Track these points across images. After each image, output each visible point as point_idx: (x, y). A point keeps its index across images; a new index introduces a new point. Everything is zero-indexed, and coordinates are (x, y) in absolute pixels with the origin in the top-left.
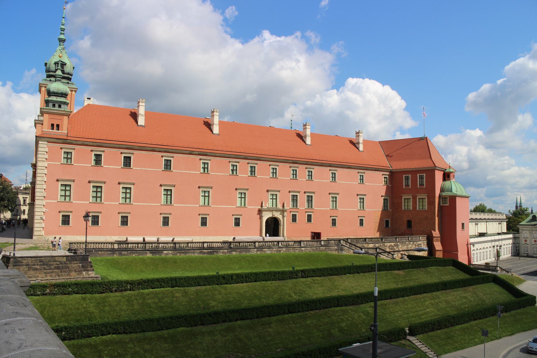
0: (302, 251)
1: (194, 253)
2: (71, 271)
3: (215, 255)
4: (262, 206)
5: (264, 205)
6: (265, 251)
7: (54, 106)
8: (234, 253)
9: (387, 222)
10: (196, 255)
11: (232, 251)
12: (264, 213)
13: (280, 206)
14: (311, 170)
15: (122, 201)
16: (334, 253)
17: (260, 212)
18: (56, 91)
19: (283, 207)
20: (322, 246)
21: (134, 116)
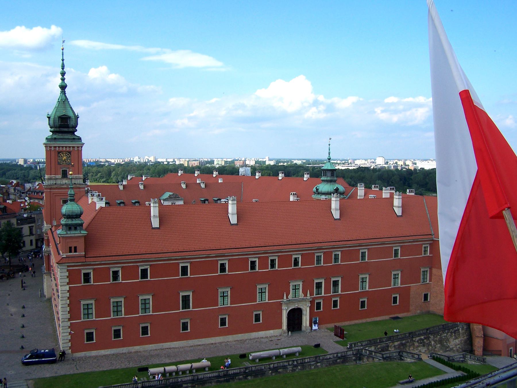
0: (318, 366)
1: (211, 383)
5: (285, 297)
6: (279, 372)
8: (249, 378)
11: (248, 376)
14: (338, 253)
18: (71, 214)
19: (306, 295)
20: (339, 358)
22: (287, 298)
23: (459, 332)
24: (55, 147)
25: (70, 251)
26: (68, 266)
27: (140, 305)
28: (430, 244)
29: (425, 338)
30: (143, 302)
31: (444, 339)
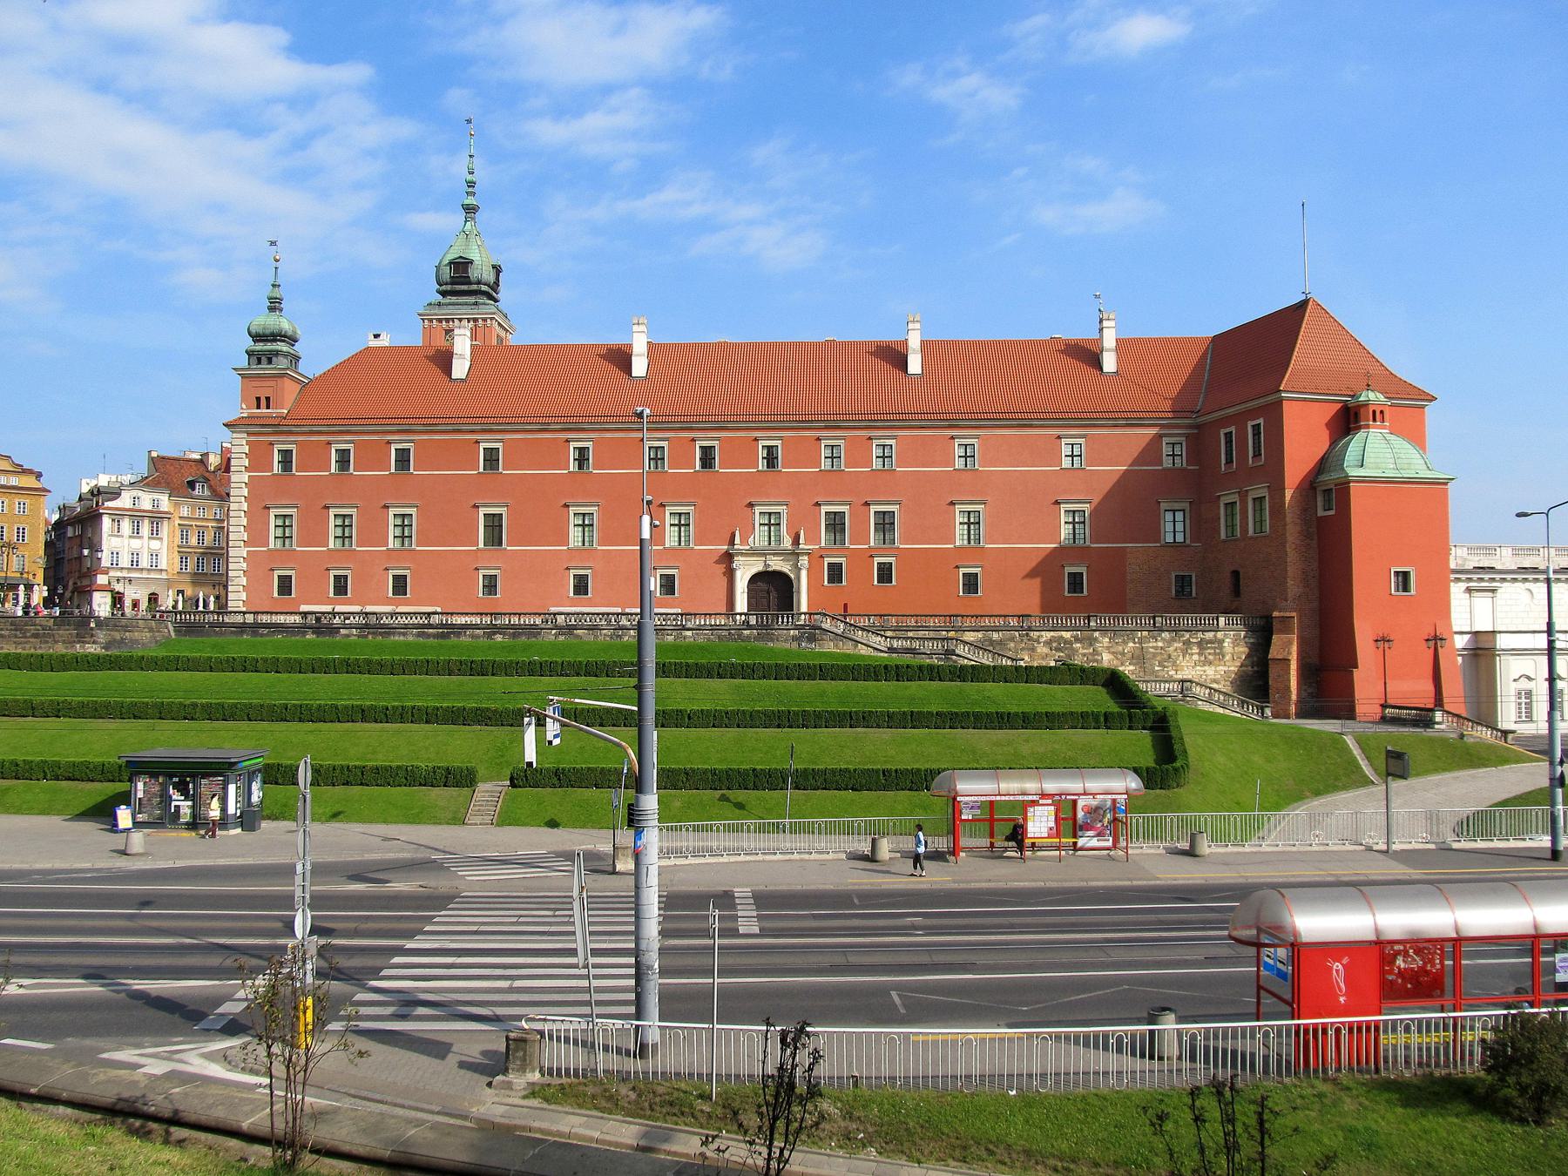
2: (56, 642)
3: (454, 639)
4: (732, 543)
5: (737, 540)
6: (578, 636)
7: (259, 361)
8: (499, 638)
9: (1183, 582)
10: (411, 638)
12: (738, 561)
13: (787, 543)
14: (888, 442)
15: (392, 543)
16: (787, 646)
17: (728, 558)
19: (796, 541)
20: (750, 627)
21: (444, 360)
22: (744, 541)
23: (1221, 648)
24: (440, 321)
25: (258, 407)
26: (249, 434)
27: (391, 528)
28: (1187, 436)
29: (1077, 640)
30: (399, 522)
31: (1155, 655)
